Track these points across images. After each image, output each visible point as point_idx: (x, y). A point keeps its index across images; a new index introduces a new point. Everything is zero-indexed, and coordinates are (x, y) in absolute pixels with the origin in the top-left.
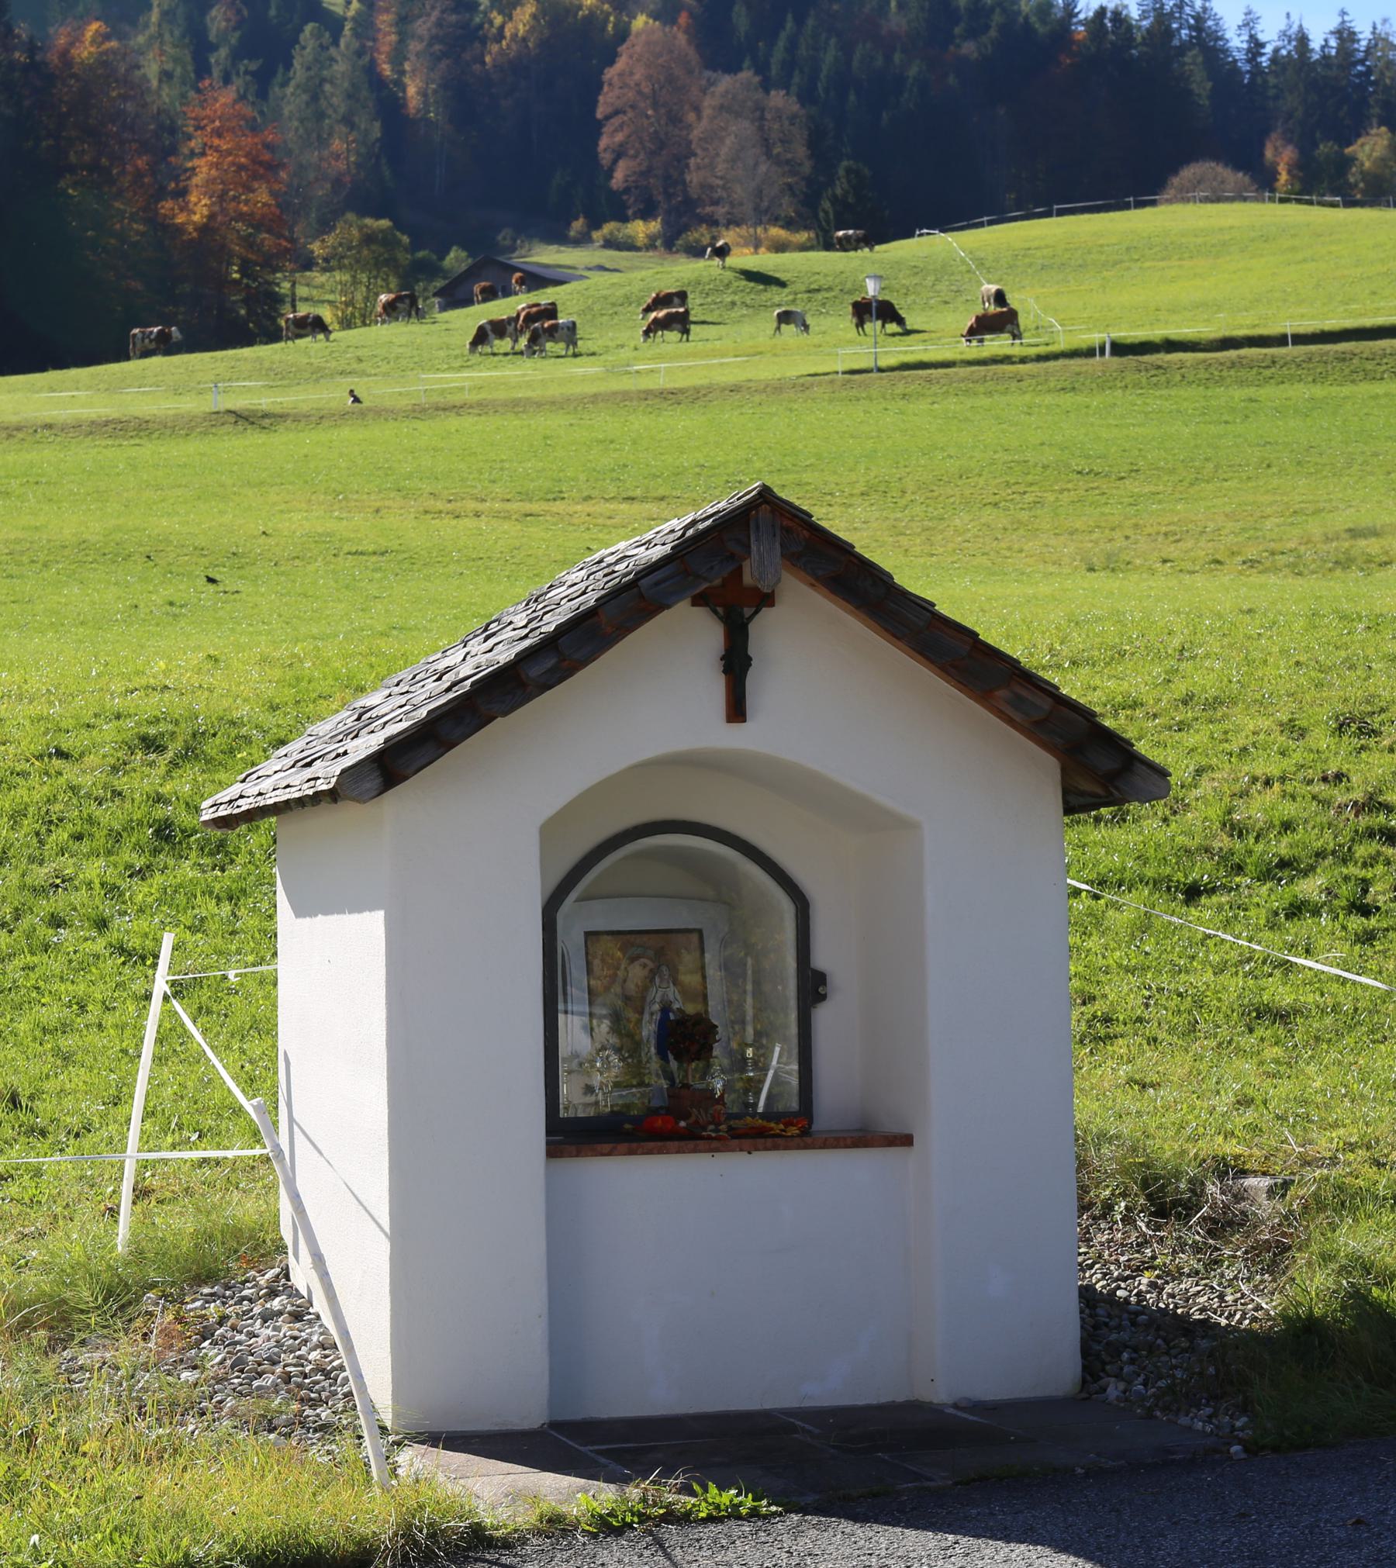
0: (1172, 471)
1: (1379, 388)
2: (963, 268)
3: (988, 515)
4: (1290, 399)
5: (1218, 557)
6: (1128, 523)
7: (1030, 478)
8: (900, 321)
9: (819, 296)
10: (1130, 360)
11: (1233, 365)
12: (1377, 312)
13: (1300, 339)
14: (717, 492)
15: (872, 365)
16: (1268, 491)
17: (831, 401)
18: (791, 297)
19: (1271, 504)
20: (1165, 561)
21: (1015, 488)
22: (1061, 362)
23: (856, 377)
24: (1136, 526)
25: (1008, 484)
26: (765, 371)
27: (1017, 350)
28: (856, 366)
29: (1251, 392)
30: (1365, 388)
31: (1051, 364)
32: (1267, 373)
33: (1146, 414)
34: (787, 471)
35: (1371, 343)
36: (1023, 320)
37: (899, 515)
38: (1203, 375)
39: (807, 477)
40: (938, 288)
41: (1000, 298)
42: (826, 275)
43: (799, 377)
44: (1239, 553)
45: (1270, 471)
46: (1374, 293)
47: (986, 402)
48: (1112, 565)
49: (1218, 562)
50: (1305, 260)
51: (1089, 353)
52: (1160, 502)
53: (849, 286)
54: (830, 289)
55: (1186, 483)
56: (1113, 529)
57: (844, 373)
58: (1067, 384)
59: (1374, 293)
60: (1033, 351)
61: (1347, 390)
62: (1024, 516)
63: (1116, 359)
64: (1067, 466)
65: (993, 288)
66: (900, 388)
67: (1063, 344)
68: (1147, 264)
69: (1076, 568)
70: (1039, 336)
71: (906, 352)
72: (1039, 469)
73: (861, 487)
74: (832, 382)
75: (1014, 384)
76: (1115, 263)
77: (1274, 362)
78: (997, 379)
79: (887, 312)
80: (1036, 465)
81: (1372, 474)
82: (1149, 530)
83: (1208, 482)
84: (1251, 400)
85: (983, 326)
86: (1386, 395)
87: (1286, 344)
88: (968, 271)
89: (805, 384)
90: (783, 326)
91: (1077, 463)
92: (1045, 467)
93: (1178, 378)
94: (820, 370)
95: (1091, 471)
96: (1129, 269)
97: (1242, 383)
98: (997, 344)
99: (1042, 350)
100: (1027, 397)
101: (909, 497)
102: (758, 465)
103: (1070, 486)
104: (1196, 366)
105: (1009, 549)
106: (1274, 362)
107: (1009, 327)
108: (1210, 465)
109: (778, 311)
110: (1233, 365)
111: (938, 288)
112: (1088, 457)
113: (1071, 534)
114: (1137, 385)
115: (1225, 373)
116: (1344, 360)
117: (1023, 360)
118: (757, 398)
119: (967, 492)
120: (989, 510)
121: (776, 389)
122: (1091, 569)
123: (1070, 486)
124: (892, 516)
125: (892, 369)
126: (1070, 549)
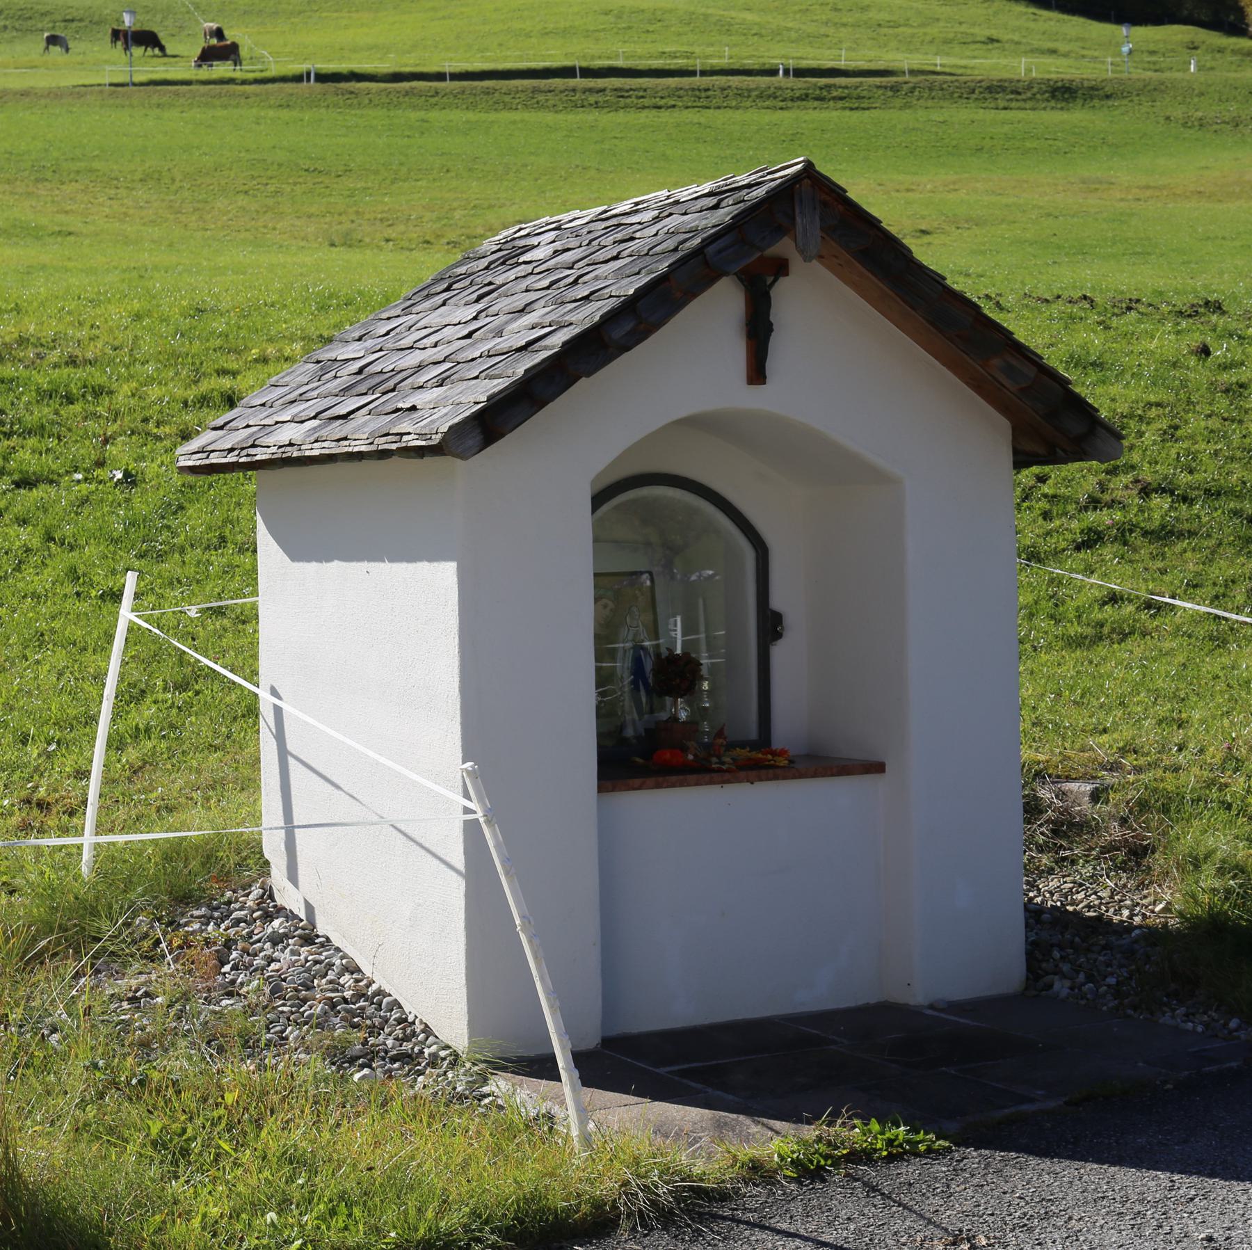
0: (376, 172)
1: (516, 116)
2: (184, 10)
3: (242, 201)
4: (453, 124)
5: (427, 238)
6: (351, 210)
7: (269, 173)
8: (162, 48)
9: (74, 25)
10: (330, 86)
11: (407, 94)
12: (506, 58)
13: (456, 77)
14: (26, 173)
15: (127, 80)
16: (450, 190)
17: (102, 106)
18: (51, 25)
19: (456, 199)
20: (388, 240)
21: (259, 180)
22: (277, 85)
23: (120, 89)
24: (357, 213)
25: (253, 177)
26: (41, 81)
27: (238, 75)
28: (115, 81)
29: (421, 114)
30: (505, 116)
31: (270, 86)
32: (433, 100)
33: (348, 127)
34: (79, 160)
35: (507, 82)
36: (244, 52)
37: (172, 198)
38: (385, 100)
39: (96, 165)
40: (166, 24)
41: (219, 33)
42: (77, 9)
43: (74, 87)
44: (443, 236)
45: (449, 175)
46: (500, 45)
47: (220, 113)
48: (349, 242)
49: (428, 242)
50: (444, 18)
51: (298, 79)
52: (371, 195)
53: (96, 18)
54: (81, 20)
55: (388, 182)
56: (340, 214)
57: (111, 85)
58: (283, 102)
59: (500, 45)
60: (251, 76)
61: (493, 116)
62: (270, 202)
63: (319, 85)
64: (297, 165)
65: (214, 26)
66: (155, 99)
67: (273, 71)
68: (324, 14)
69: (321, 244)
70: (253, 64)
71: (152, 72)
72: (276, 167)
73: (138, 176)
74: (101, 92)
75: (243, 101)
76: (300, 13)
77: (437, 93)
78: (232, 95)
79: (147, 39)
80: (272, 163)
81: (524, 179)
82: (367, 216)
83: (404, 181)
84: (423, 121)
85: (207, 56)
86: (522, 121)
87: (445, 79)
88: (188, 12)
89: (80, 92)
90: (51, 47)
91: (307, 164)
92: (280, 165)
93: (367, 101)
94: (87, 82)
95: (315, 170)
96: (310, 17)
97: (414, 107)
98: (222, 69)
99: (258, 75)
100: (254, 110)
101: (178, 184)
102: (55, 154)
103: (301, 180)
104: (380, 92)
105: (265, 227)
106: (437, 93)
107: (233, 57)
108: (404, 169)
109: (46, 35)
110: (407, 94)
111: (166, 24)
112: (312, 159)
113: (309, 217)
114: (336, 105)
115: (401, 99)
116: (488, 93)
117: (244, 82)
118: (43, 102)
119: (223, 183)
120: (241, 196)
121: (55, 95)
122: (333, 245)
123: (301, 180)
124: (167, 198)
125: (142, 84)
126: (311, 229)
